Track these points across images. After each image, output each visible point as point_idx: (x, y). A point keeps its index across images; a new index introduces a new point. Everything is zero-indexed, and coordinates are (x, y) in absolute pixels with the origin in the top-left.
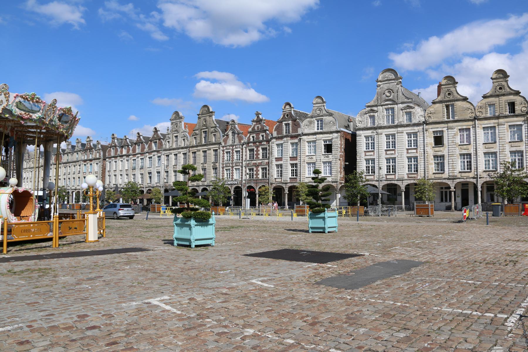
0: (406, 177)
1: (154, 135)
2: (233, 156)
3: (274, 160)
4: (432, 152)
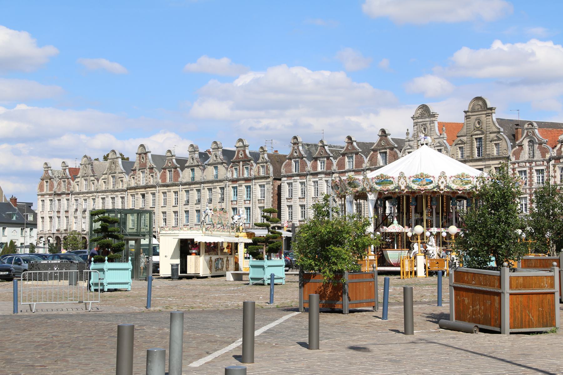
1: (380, 140)
2: (531, 177)
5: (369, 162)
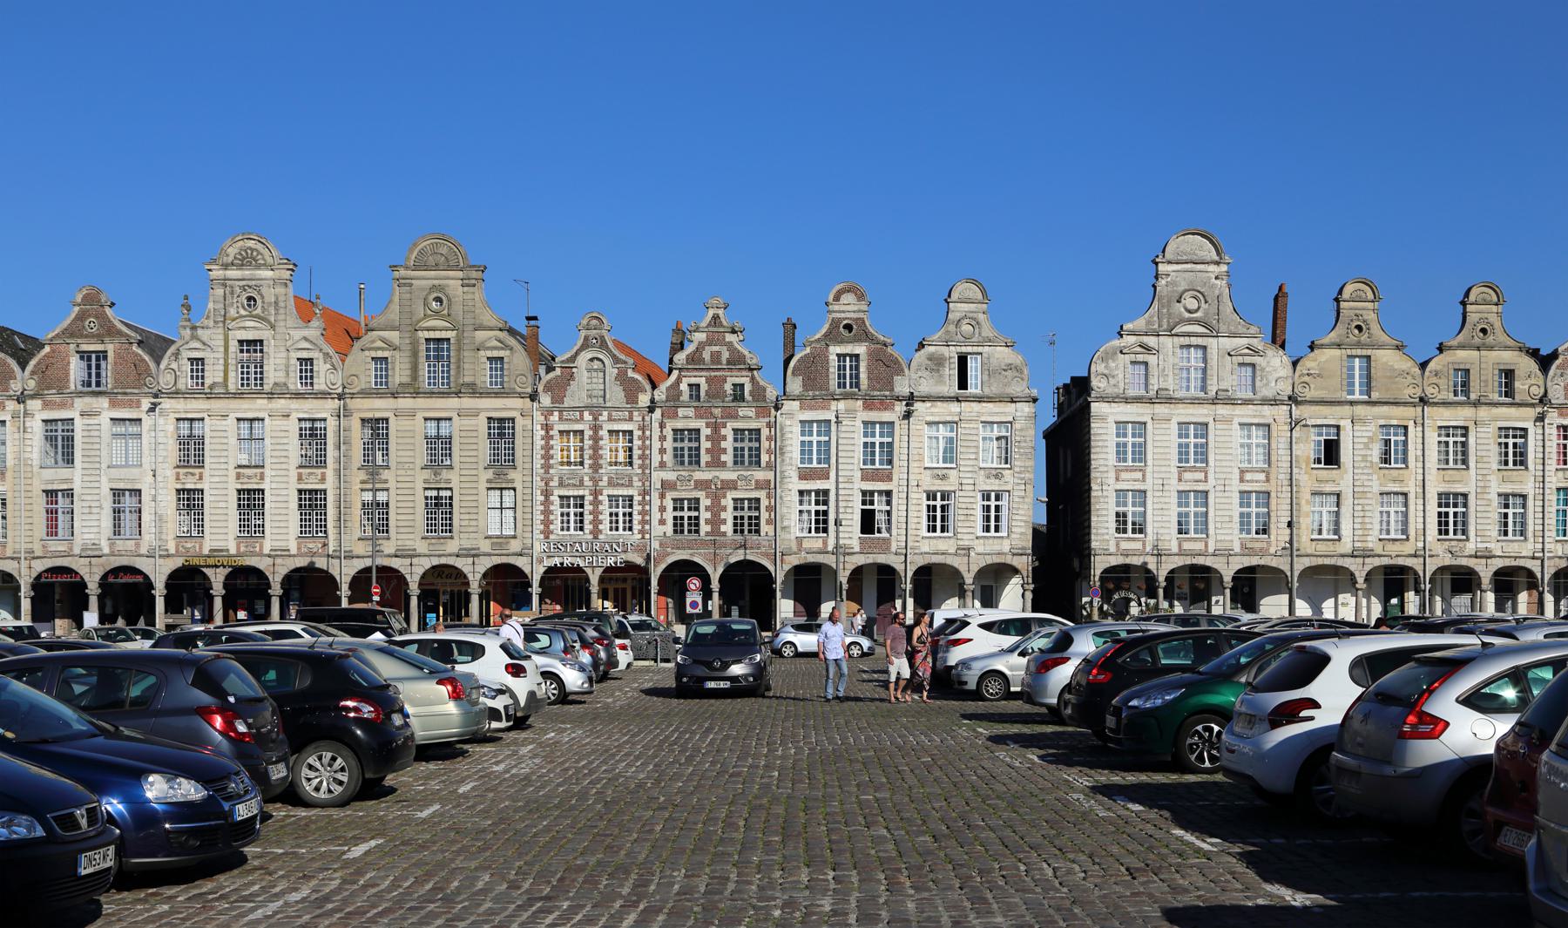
0: (1237, 549)
3: (794, 475)
5: (35, 377)
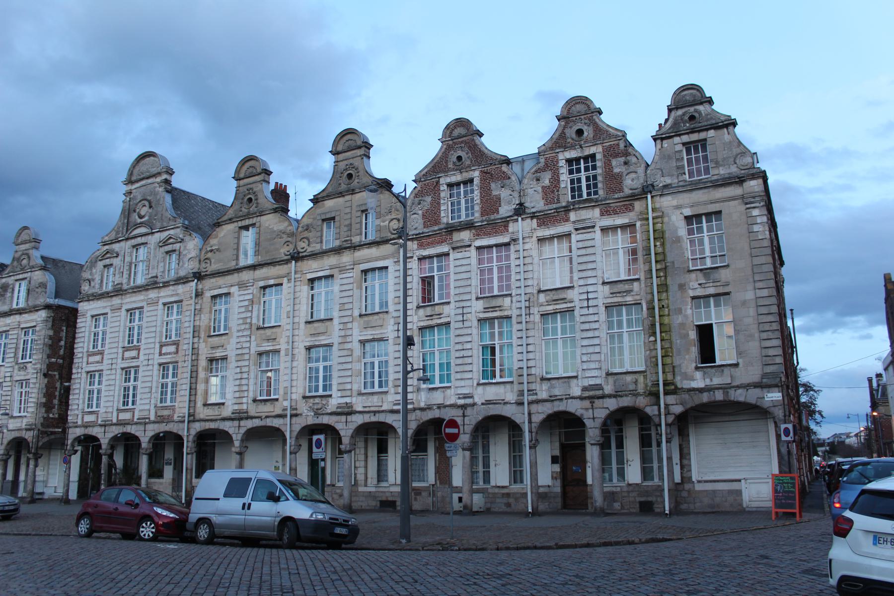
0: (152, 418)
4: (205, 351)
